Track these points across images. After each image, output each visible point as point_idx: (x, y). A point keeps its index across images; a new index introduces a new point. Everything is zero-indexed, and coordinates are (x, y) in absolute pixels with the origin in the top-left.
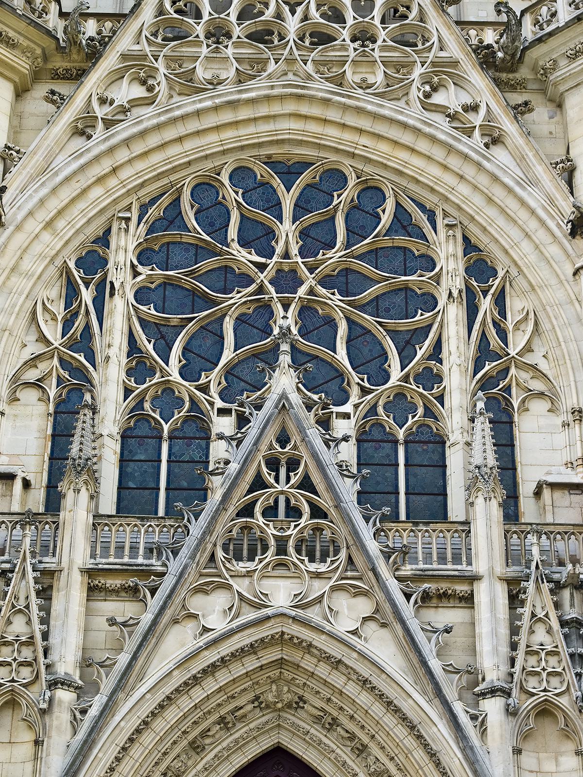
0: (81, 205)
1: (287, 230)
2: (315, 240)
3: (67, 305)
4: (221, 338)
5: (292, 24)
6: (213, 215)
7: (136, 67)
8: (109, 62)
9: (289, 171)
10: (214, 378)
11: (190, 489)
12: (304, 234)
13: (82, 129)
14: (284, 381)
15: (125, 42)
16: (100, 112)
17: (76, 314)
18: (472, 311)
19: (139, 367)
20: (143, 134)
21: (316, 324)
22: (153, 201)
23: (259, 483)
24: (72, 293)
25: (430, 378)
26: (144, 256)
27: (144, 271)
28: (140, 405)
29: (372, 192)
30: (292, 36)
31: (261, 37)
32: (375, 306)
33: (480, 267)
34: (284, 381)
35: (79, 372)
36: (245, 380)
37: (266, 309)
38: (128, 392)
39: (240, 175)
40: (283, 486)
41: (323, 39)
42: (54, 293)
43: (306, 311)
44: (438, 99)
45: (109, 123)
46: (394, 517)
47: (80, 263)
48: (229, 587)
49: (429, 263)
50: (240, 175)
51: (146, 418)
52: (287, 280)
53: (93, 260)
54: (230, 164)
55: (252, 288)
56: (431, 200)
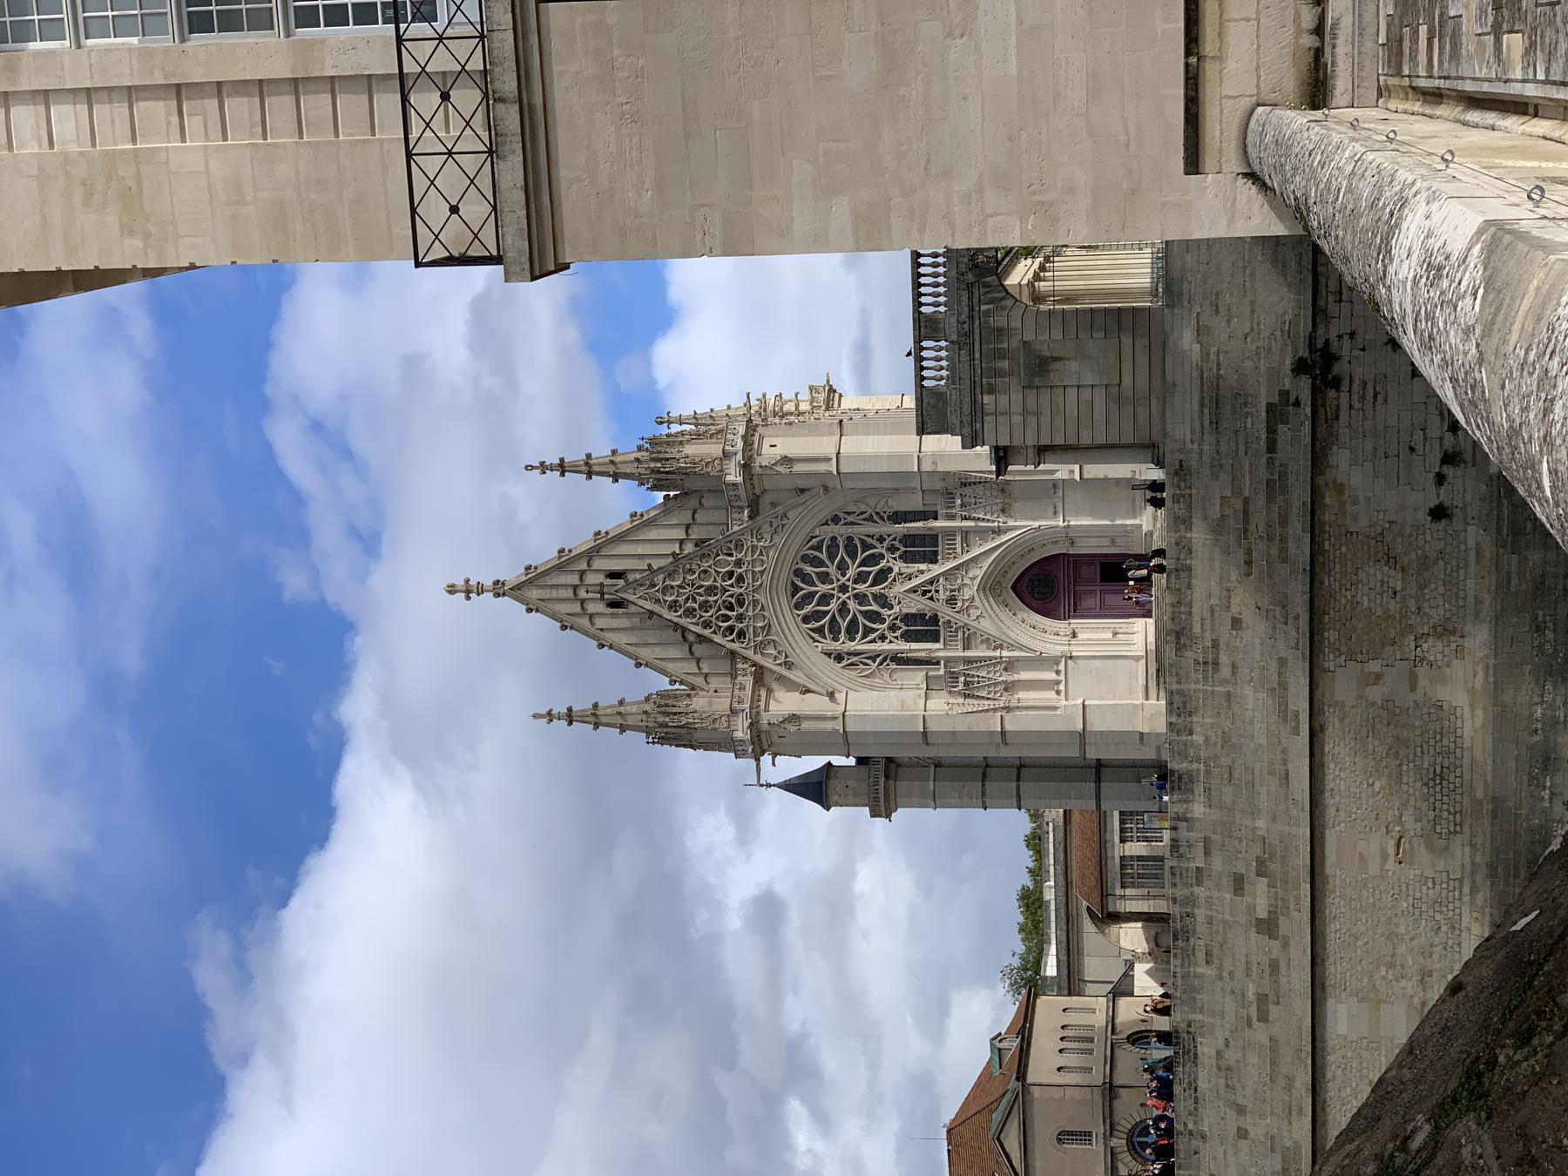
1: (823, 588)
2: (825, 578)
5: (737, 590)
7: (760, 647)
8: (758, 658)
10: (885, 612)
13: (789, 665)
15: (750, 653)
18: (852, 523)
19: (883, 638)
23: (931, 598)
25: (881, 539)
26: (836, 639)
31: (741, 603)
32: (853, 557)
33: (836, 520)
35: (885, 659)
36: (883, 600)
37: (856, 596)
39: (798, 606)
41: (740, 579)
49: (834, 539)
52: (843, 589)
53: (839, 658)
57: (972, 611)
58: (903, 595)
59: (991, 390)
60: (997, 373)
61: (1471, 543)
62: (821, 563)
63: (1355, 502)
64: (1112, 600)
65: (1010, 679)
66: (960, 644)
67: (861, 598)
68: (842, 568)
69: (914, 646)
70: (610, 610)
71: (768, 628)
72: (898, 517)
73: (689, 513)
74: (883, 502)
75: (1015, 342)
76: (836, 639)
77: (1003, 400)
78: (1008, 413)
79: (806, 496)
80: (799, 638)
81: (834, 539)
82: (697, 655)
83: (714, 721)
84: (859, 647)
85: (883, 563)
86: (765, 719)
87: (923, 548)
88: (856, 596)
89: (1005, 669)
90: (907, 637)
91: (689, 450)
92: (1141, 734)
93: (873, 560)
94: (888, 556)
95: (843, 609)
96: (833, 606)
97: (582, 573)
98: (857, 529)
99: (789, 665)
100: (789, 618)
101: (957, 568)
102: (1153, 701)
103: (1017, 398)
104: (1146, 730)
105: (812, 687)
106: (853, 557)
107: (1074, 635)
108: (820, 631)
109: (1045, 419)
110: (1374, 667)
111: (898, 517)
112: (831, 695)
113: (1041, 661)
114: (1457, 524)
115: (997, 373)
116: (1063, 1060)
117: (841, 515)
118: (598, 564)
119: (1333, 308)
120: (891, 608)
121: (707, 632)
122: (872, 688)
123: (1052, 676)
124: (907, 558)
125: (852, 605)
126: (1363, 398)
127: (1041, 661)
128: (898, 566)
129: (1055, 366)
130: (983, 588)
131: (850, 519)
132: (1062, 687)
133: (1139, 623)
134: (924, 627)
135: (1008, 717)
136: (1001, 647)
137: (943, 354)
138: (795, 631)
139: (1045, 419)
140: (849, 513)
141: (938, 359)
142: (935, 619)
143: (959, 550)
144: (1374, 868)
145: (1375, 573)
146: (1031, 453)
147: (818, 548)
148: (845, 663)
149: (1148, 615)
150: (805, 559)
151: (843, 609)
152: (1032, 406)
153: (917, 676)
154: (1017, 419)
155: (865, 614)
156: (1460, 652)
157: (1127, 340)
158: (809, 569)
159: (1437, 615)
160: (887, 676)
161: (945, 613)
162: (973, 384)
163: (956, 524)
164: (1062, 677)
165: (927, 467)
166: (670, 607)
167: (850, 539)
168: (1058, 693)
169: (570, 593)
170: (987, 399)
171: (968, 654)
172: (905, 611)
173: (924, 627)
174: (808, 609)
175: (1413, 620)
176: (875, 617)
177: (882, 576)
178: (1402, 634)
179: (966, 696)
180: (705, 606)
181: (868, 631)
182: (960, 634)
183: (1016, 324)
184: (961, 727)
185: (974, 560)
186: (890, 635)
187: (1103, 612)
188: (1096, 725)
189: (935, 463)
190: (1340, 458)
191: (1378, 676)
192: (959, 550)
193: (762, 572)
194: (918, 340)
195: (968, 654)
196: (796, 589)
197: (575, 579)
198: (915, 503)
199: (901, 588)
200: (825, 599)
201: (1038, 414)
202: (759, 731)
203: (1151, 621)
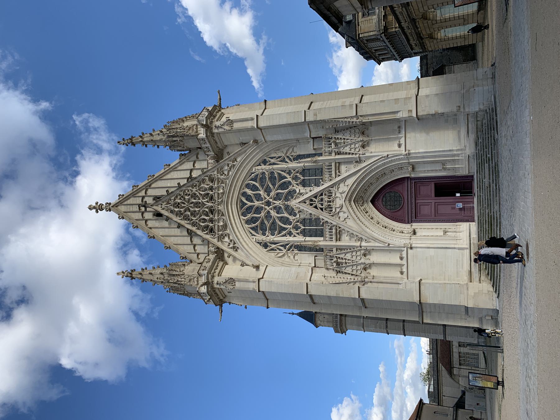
0: (253, 249)
1: (257, 203)
2: (259, 198)
3: (276, 250)
4: (282, 217)
5: (210, 204)
6: (253, 220)
7: (221, 238)
8: (219, 244)
10: (291, 218)
12: (258, 201)
13: (235, 249)
14: (294, 203)
15: (215, 241)
16: (231, 246)
17: (278, 248)
18: (274, 164)
19: (290, 234)
20: (237, 236)
21: (278, 197)
22: (251, 233)
23: (316, 207)
24: (272, 250)
26: (264, 234)
27: (267, 234)
28: (298, 233)
30: (212, 204)
31: (212, 212)
33: (265, 162)
34: (294, 203)
35: (291, 247)
36: (292, 212)
37: (275, 208)
38: (295, 236)
40: (317, 202)
41: (212, 198)
42: (273, 254)
43: (275, 199)
44: (226, 173)
45: (235, 243)
46: (322, 179)
47: (266, 248)
48: (338, 213)
49: (263, 173)
50: (244, 214)
51: (301, 232)
52: (268, 203)
53: (265, 246)
54: (242, 217)
55: (270, 211)
56: (249, 174)
57: (341, 214)
64: (443, 209)
65: (367, 262)
66: (334, 237)
69: (308, 239)
70: (155, 217)
71: (225, 227)
72: (299, 157)
73: (192, 163)
74: (291, 150)
79: (246, 145)
80: (242, 232)
81: (263, 173)
82: (194, 243)
83: (190, 280)
84: (275, 239)
85: (290, 187)
86: (216, 279)
87: (311, 176)
88: (275, 208)
89: (365, 255)
90: (304, 233)
91: (186, 124)
92: (467, 308)
93: (285, 186)
94: (293, 182)
97: (143, 197)
98: (275, 166)
99: (235, 249)
100: (238, 221)
101: (332, 186)
102: (475, 283)
104: (470, 305)
105: (248, 262)
106: (274, 185)
107: (414, 233)
112: (257, 267)
113: (388, 249)
117: (268, 159)
118: (150, 192)
120: (295, 215)
121: (194, 229)
122: (283, 264)
123: (398, 261)
125: (273, 213)
127: (388, 249)
128: (299, 189)
131: (273, 161)
132: (405, 270)
133: (464, 226)
134: (313, 227)
136: (361, 239)
138: (241, 229)
140: (272, 158)
143: (334, 175)
147: (254, 179)
148: (268, 249)
149: (470, 219)
150: (248, 186)
153: (307, 259)
155: (281, 219)
158: (249, 192)
160: (292, 257)
161: (324, 216)
163: (333, 157)
164: (404, 262)
166: (177, 215)
167: (272, 173)
168: (402, 273)
169: (136, 208)
171: (338, 243)
172: (302, 217)
173: (313, 227)
174: (249, 216)
179: (338, 272)
180: (193, 214)
182: (334, 231)
184: (332, 293)
185: (344, 180)
186: (294, 232)
187: (437, 218)
188: (430, 298)
189: (315, 115)
192: (334, 175)
193: (223, 193)
195: (338, 243)
196: (244, 204)
197: (139, 201)
202: (213, 288)
203: (474, 223)
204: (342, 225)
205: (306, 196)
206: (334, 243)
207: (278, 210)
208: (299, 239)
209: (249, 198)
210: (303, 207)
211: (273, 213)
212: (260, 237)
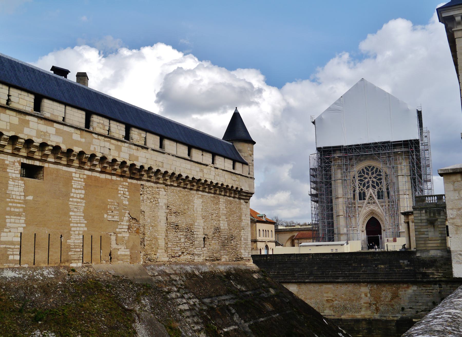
1: (370, 173)
2: (373, 174)
9: (370, 167)
10: (365, 188)
11: (364, 199)
19: (359, 187)
26: (358, 177)
29: (377, 169)
32: (378, 180)
36: (368, 187)
39: (366, 168)
43: (372, 181)
52: (370, 178)
58: (370, 192)
59: (426, 212)
60: (430, 214)
61: (397, 315)
62: (376, 172)
63: (405, 291)
67: (368, 182)
68: (375, 178)
69: (358, 195)
75: (437, 217)
76: (358, 177)
77: (424, 215)
78: (421, 216)
85: (377, 187)
90: (360, 193)
93: (377, 184)
95: (365, 178)
96: (366, 176)
98: (384, 180)
100: (363, 166)
103: (424, 218)
107: (363, 231)
108: (360, 173)
109: (420, 224)
110: (369, 295)
111: (388, 189)
114: (401, 312)
115: (430, 214)
116: (261, 230)
119: (449, 286)
120: (367, 189)
124: (378, 192)
125: (366, 180)
126: (428, 292)
129: (432, 227)
130: (372, 210)
134: (362, 196)
135: (343, 217)
137: (434, 201)
139: (420, 224)
141: (432, 200)
142: (364, 199)
144: (325, 295)
145: (390, 296)
146: (407, 221)
150: (377, 169)
151: (365, 178)
152: (423, 221)
154: (420, 218)
155: (365, 183)
156: (372, 312)
157: (439, 242)
158: (375, 169)
159: (381, 308)
161: (366, 201)
162: (427, 208)
165: (401, 196)
170: (424, 211)
175: (379, 303)
176: (364, 185)
177: (374, 187)
178: (376, 301)
181: (361, 184)
183: (442, 217)
190: (415, 288)
191: (367, 296)
194: (437, 196)
198: (392, 193)
199: (371, 190)
200: (368, 174)
201: (421, 222)
204: (363, 208)
205: (373, 194)
206: (357, 206)
207: (368, 182)
208: (357, 191)
209: (372, 169)
210: (369, 193)
211: (366, 180)
212: (357, 175)
